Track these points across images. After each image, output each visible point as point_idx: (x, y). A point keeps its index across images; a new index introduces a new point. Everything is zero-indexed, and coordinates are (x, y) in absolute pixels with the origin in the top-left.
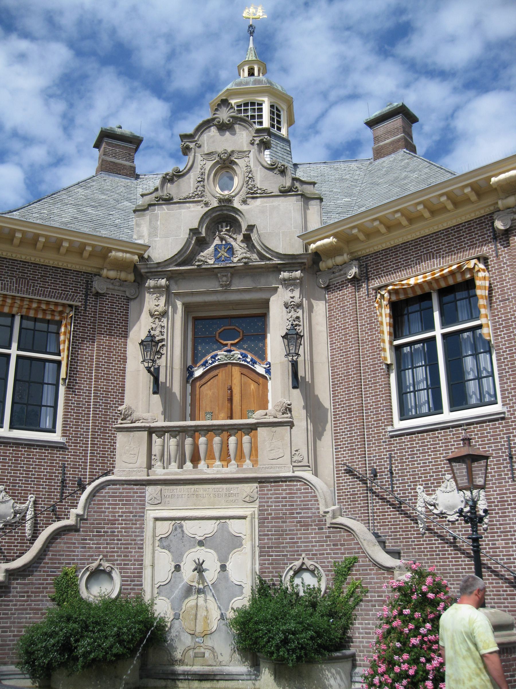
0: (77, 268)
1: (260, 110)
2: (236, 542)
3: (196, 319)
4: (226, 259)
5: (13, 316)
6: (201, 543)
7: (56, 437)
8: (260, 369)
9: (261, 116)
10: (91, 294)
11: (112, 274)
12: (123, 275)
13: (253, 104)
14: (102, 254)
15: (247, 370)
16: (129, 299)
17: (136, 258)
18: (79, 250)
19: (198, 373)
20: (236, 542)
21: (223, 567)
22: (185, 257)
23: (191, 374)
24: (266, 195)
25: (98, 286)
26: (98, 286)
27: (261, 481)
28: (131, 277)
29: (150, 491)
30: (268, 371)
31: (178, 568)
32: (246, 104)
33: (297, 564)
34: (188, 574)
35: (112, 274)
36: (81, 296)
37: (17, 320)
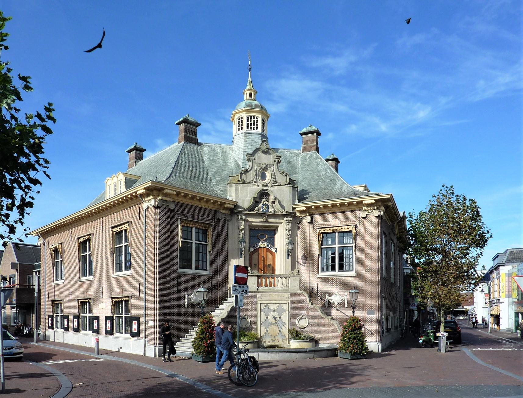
0: (212, 208)
1: (257, 122)
2: (284, 311)
3: (250, 230)
4: (266, 211)
5: (192, 228)
6: (274, 311)
7: (207, 272)
8: (273, 250)
9: (257, 125)
10: (216, 219)
11: (224, 211)
12: (227, 212)
13: (254, 118)
14: (222, 204)
15: (268, 250)
16: (228, 221)
17: (233, 206)
18: (215, 202)
19: (252, 250)
20: (284, 311)
21: (280, 317)
22: (252, 208)
23: (249, 250)
24: (280, 185)
25: (219, 216)
26: (219, 216)
27: (291, 293)
28: (229, 213)
29: (258, 295)
30: (276, 251)
31: (267, 317)
32: (251, 117)
33: (300, 317)
34: (271, 319)
35: (224, 211)
36: (212, 220)
37: (194, 229)
